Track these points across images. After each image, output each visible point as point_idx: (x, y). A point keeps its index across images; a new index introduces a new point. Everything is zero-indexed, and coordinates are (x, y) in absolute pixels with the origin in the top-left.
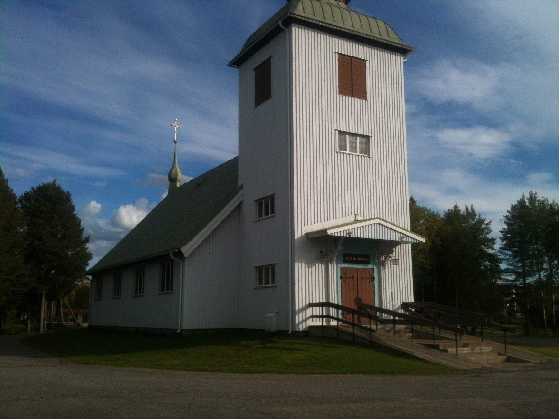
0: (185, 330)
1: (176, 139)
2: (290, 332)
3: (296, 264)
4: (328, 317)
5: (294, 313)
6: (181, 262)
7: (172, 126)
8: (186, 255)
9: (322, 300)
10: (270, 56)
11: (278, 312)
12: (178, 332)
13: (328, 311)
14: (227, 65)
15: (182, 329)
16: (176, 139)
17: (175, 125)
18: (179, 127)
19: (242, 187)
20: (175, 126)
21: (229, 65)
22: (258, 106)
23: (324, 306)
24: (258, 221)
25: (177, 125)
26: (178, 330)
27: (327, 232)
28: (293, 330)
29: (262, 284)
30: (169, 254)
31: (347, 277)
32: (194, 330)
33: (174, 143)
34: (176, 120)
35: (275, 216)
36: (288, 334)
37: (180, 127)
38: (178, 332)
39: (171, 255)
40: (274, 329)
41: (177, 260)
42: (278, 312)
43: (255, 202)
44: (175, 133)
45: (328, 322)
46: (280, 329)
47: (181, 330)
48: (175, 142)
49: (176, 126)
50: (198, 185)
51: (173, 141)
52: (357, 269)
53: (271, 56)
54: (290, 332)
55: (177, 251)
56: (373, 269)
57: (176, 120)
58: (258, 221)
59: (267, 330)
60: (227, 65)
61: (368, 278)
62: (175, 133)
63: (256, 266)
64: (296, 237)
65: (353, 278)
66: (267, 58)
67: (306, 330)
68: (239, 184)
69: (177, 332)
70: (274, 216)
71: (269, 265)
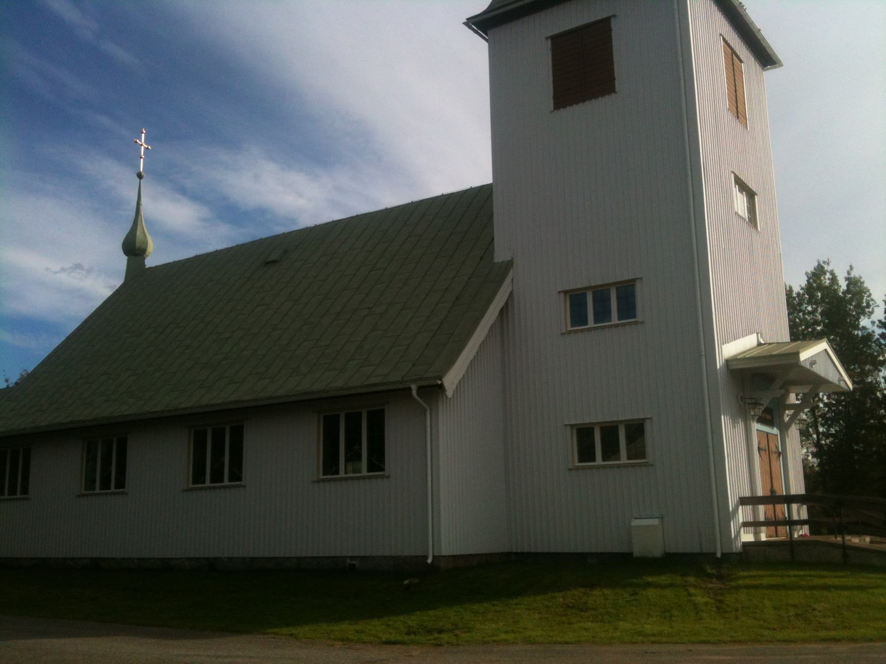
0: (445, 556)
1: (141, 170)
2: (719, 555)
3: (723, 417)
4: (791, 523)
5: (727, 517)
6: (428, 409)
7: (136, 142)
8: (449, 393)
9: (747, 494)
10: (610, 14)
11: (662, 518)
12: (429, 561)
13: (755, 513)
14: (464, 23)
15: (436, 554)
16: (141, 170)
17: (141, 142)
18: (148, 148)
19: (508, 265)
20: (142, 145)
21: (466, 24)
22: (565, 107)
23: (794, 503)
24: (570, 332)
25: (145, 142)
26: (426, 557)
27: (798, 358)
28: (726, 551)
29: (594, 460)
30: (410, 389)
31: (762, 449)
32: (486, 555)
33: (138, 180)
34: (142, 133)
35: (642, 323)
36: (718, 558)
37: (149, 147)
38: (429, 561)
39: (414, 393)
40: (658, 552)
41: (423, 403)
42: (662, 518)
43: (562, 295)
44: (141, 157)
45: (756, 534)
46: (672, 549)
47: (434, 557)
48: (140, 176)
49: (144, 144)
50: (274, 262)
51: (137, 172)
52: (767, 434)
53: (614, 16)
54: (719, 555)
55: (439, 382)
56: (777, 435)
57: (142, 133)
58: (570, 332)
59: (637, 552)
60: (464, 23)
61: (775, 453)
62: (141, 157)
63: (572, 423)
64: (718, 367)
65: (765, 450)
66: (605, 16)
67: (742, 551)
68: (500, 256)
69: (427, 563)
70: (636, 323)
71: (621, 422)
